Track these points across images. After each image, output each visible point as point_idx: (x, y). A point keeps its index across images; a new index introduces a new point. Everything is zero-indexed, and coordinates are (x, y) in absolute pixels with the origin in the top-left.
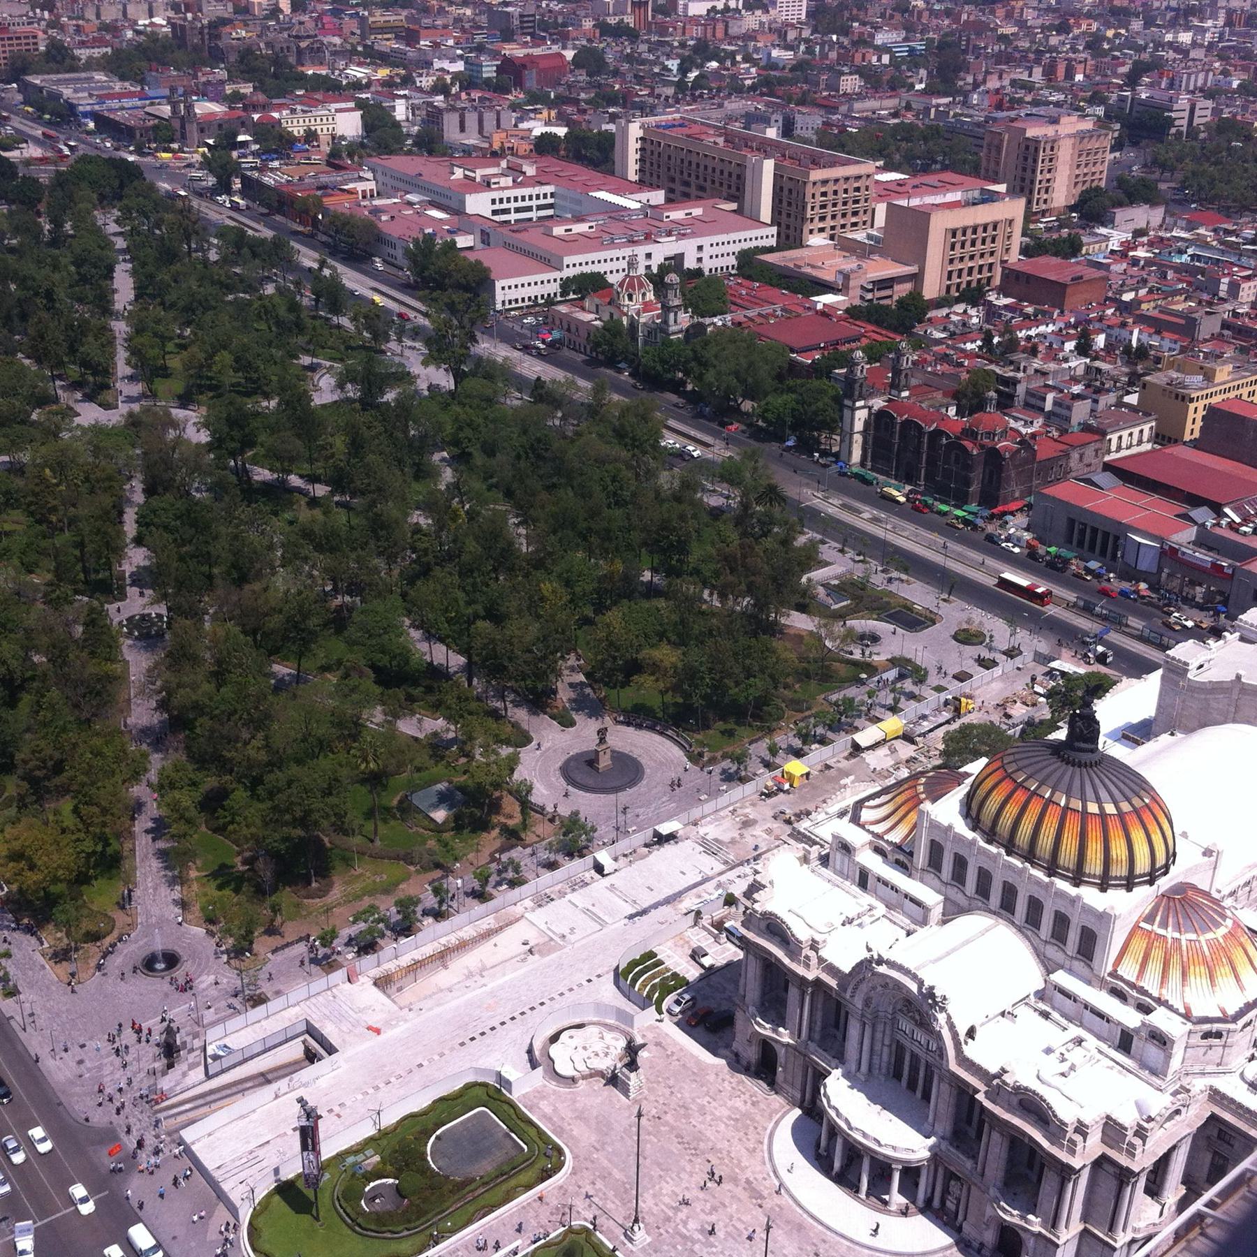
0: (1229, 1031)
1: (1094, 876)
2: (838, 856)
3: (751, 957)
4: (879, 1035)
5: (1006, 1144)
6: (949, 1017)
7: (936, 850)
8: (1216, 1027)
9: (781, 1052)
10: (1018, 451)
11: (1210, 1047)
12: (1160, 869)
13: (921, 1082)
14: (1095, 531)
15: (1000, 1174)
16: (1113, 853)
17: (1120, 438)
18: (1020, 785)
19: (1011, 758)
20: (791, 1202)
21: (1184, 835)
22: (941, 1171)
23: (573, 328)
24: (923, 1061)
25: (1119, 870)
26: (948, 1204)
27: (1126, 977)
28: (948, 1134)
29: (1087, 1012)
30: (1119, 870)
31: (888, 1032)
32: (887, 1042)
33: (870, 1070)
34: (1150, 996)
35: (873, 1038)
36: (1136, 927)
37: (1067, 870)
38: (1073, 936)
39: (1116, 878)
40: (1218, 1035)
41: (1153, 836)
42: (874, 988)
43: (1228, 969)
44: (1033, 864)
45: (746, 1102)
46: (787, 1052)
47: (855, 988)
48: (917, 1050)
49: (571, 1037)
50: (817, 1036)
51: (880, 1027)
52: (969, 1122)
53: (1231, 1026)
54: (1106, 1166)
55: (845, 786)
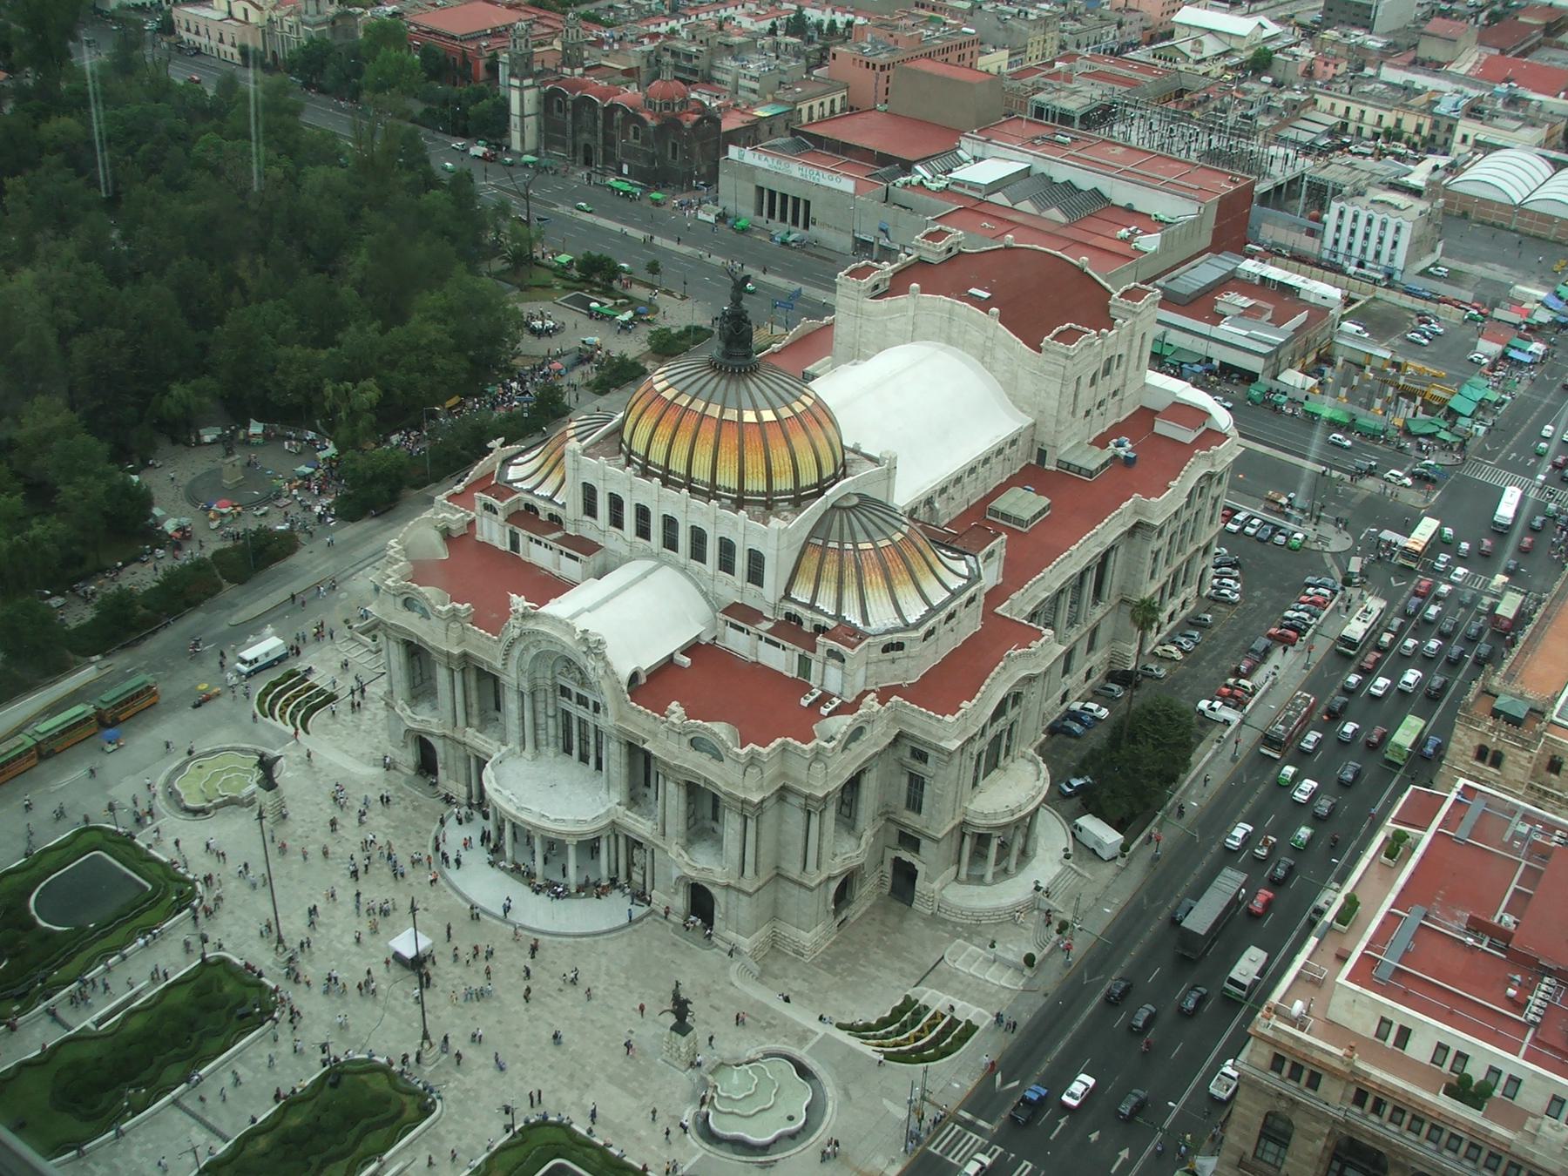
0: (911, 640)
1: (759, 494)
2: (485, 520)
3: (392, 643)
4: (540, 706)
5: (682, 793)
6: (608, 664)
7: (589, 492)
8: (896, 638)
9: (438, 745)
10: (700, 121)
11: (893, 661)
12: (828, 479)
13: (592, 750)
14: (784, 197)
15: (682, 827)
16: (775, 467)
17: (811, 108)
18: (670, 404)
19: (662, 376)
20: (460, 900)
21: (856, 451)
22: (622, 841)
23: (202, 30)
24: (591, 727)
25: (783, 483)
26: (635, 876)
27: (800, 599)
28: (625, 800)
29: (762, 643)
30: (783, 483)
31: (550, 701)
32: (551, 712)
33: (536, 747)
34: (826, 615)
35: (534, 711)
36: (807, 543)
37: (728, 490)
38: (741, 562)
39: (781, 493)
40: (899, 646)
41: (818, 443)
42: (526, 649)
43: (906, 576)
44: (691, 490)
45: (406, 808)
46: (445, 745)
47: (507, 654)
48: (584, 716)
49: (200, 767)
50: (475, 721)
51: (540, 696)
52: (647, 784)
53: (914, 634)
54: (792, 799)
55: (491, 450)
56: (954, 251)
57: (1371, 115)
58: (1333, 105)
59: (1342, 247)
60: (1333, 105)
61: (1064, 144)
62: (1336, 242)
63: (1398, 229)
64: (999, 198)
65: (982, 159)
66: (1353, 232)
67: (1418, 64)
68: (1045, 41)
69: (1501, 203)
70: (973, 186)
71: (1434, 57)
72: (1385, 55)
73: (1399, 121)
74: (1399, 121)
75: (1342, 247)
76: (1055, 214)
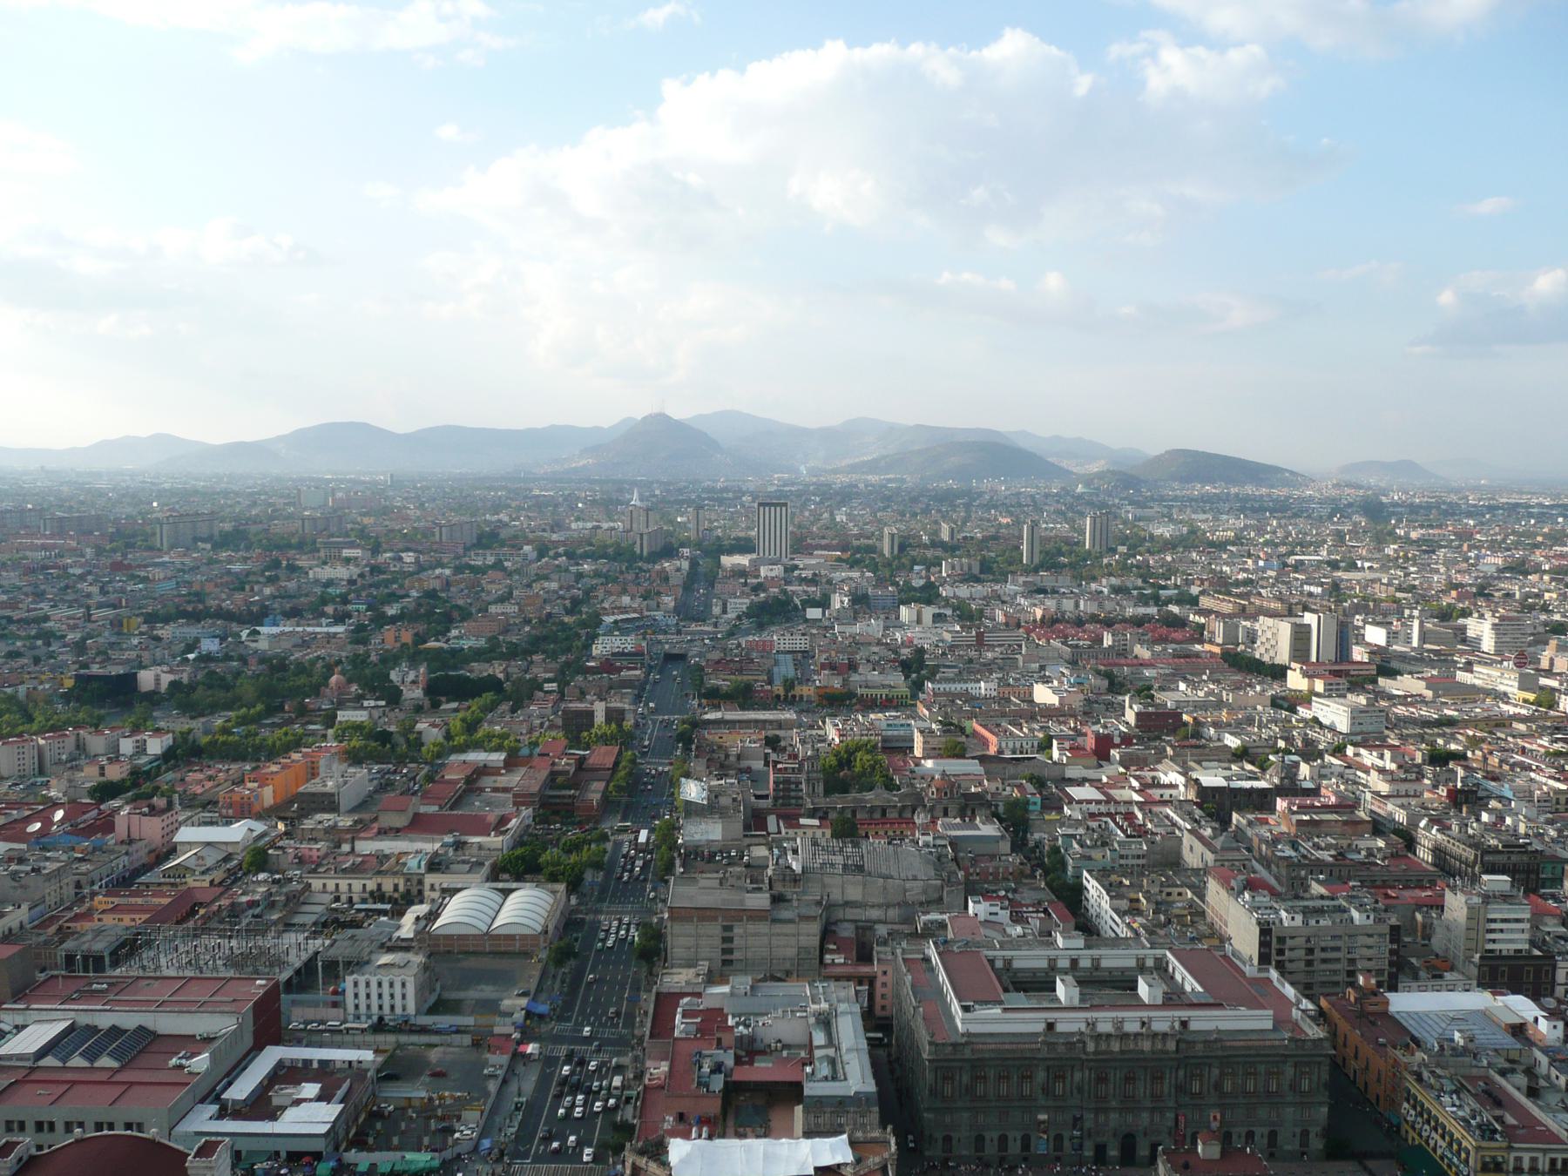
56: (25, 1159)
57: (357, 885)
58: (324, 885)
59: (363, 1009)
60: (324, 885)
61: (101, 991)
62: (357, 1007)
63: (403, 985)
64: (49, 1061)
65: (24, 1027)
66: (368, 996)
67: (383, 833)
68: (61, 888)
69: (474, 936)
70: (20, 1057)
71: (392, 825)
72: (355, 833)
73: (379, 886)
74: (379, 886)
75: (363, 1009)
76: (106, 1061)
